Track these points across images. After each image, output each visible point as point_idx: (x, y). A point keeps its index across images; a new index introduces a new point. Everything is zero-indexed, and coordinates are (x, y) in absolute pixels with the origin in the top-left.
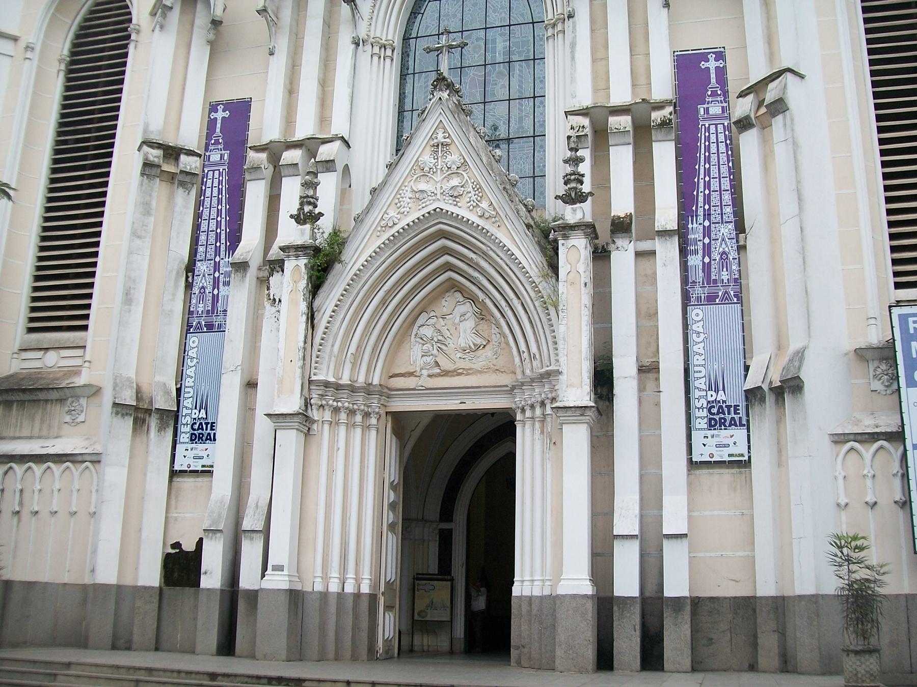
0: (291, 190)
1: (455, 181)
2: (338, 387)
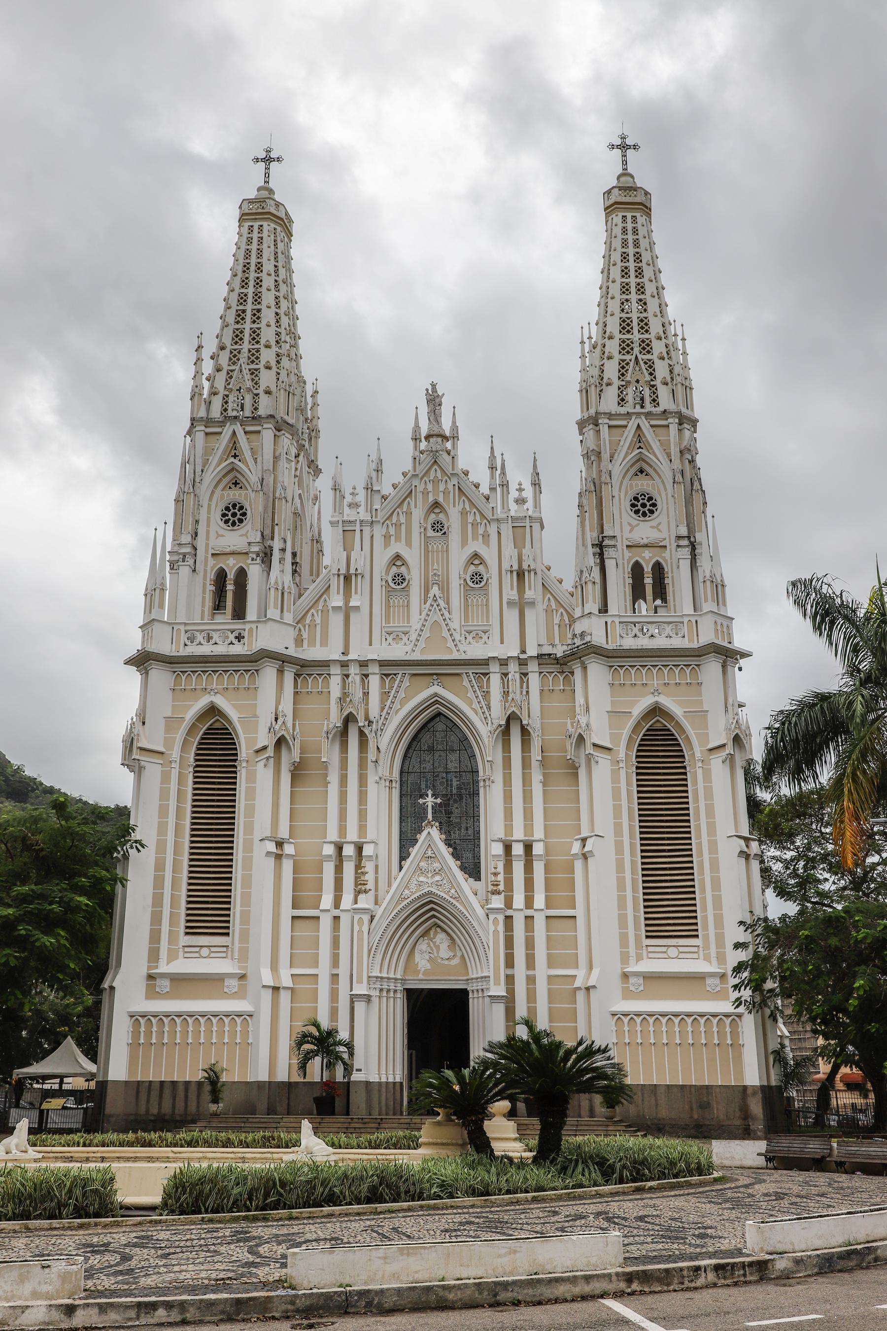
0: (349, 869)
1: (437, 878)
2: (382, 978)
